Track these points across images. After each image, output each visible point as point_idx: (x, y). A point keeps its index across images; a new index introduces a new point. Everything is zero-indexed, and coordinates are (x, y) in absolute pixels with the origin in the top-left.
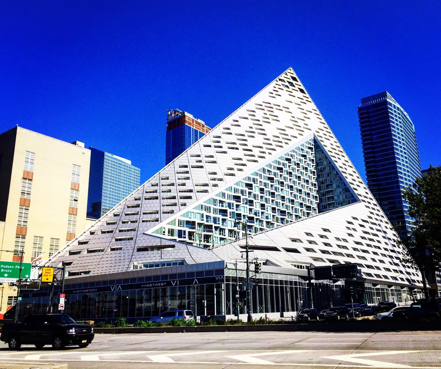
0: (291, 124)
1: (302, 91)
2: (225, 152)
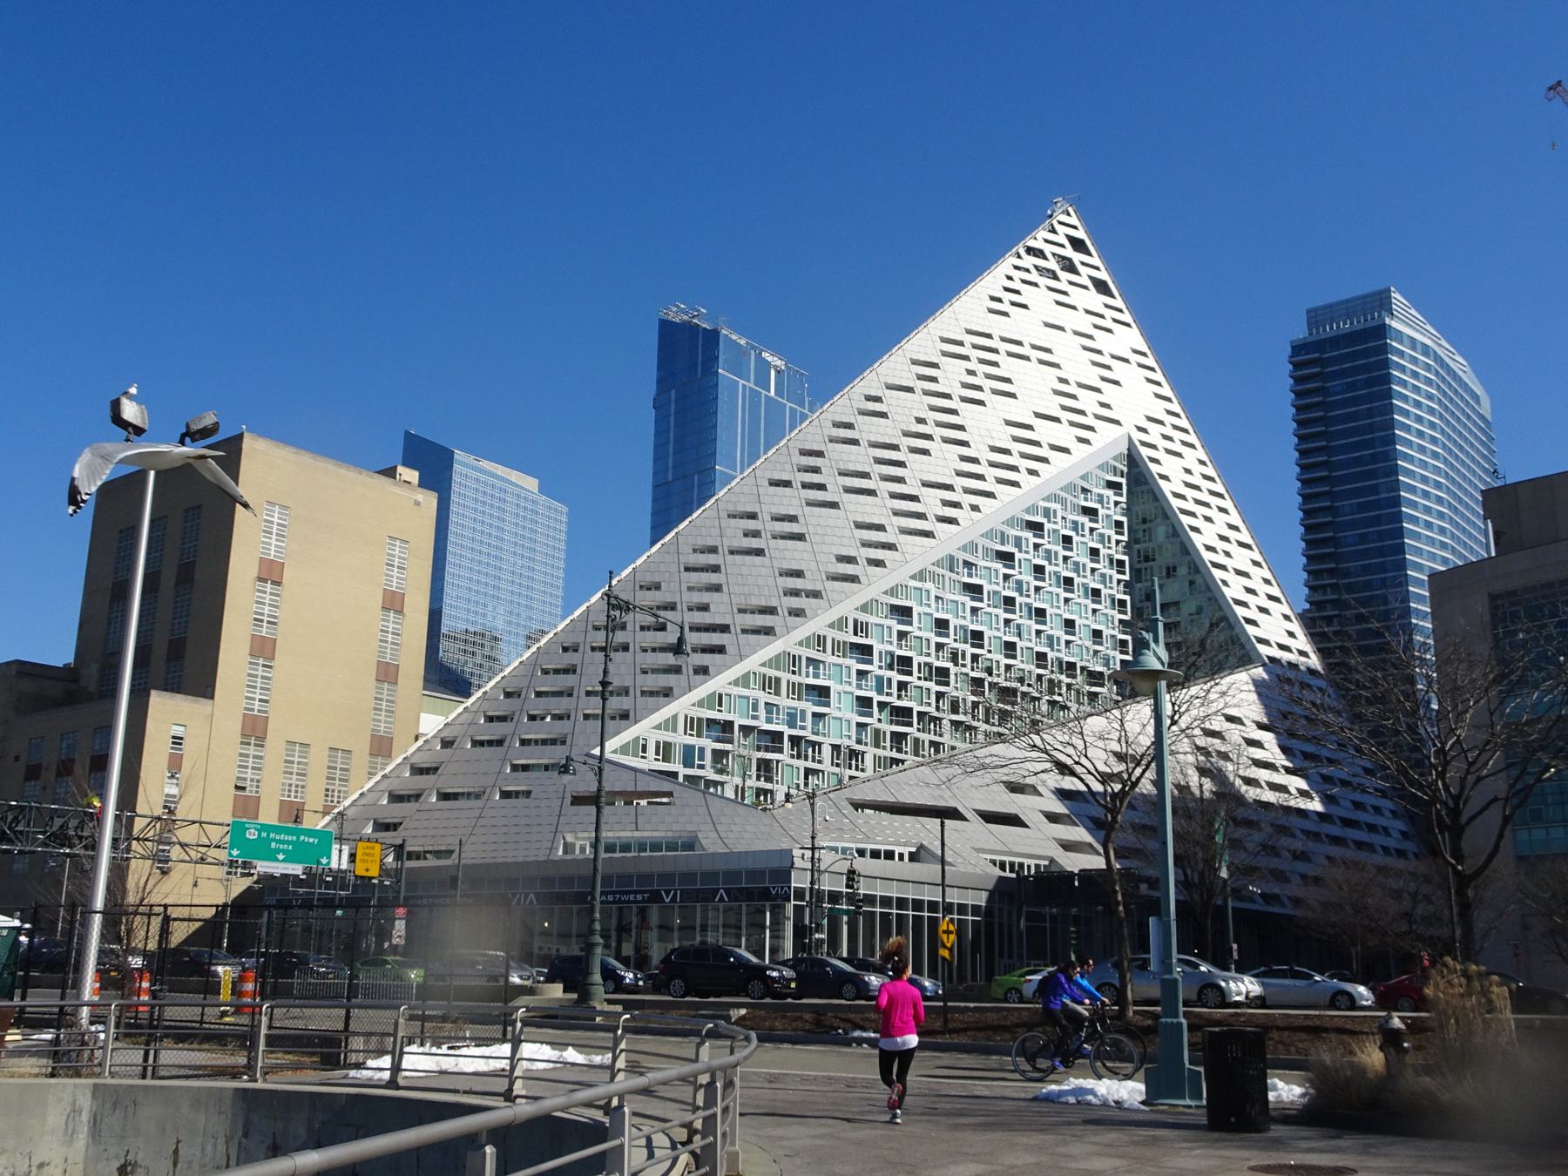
0: (1052, 406)
1: (1101, 287)
2: (834, 505)
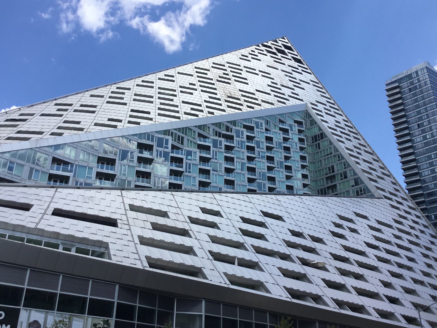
2: (125, 104)
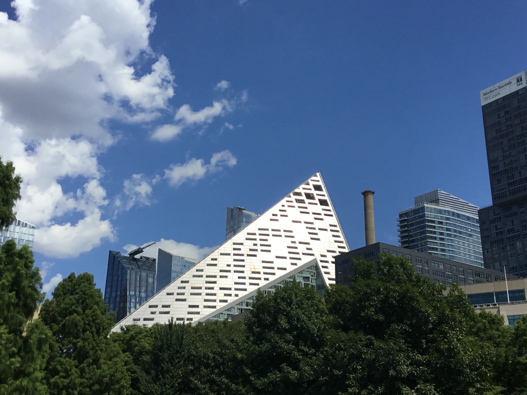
1: (323, 203)
